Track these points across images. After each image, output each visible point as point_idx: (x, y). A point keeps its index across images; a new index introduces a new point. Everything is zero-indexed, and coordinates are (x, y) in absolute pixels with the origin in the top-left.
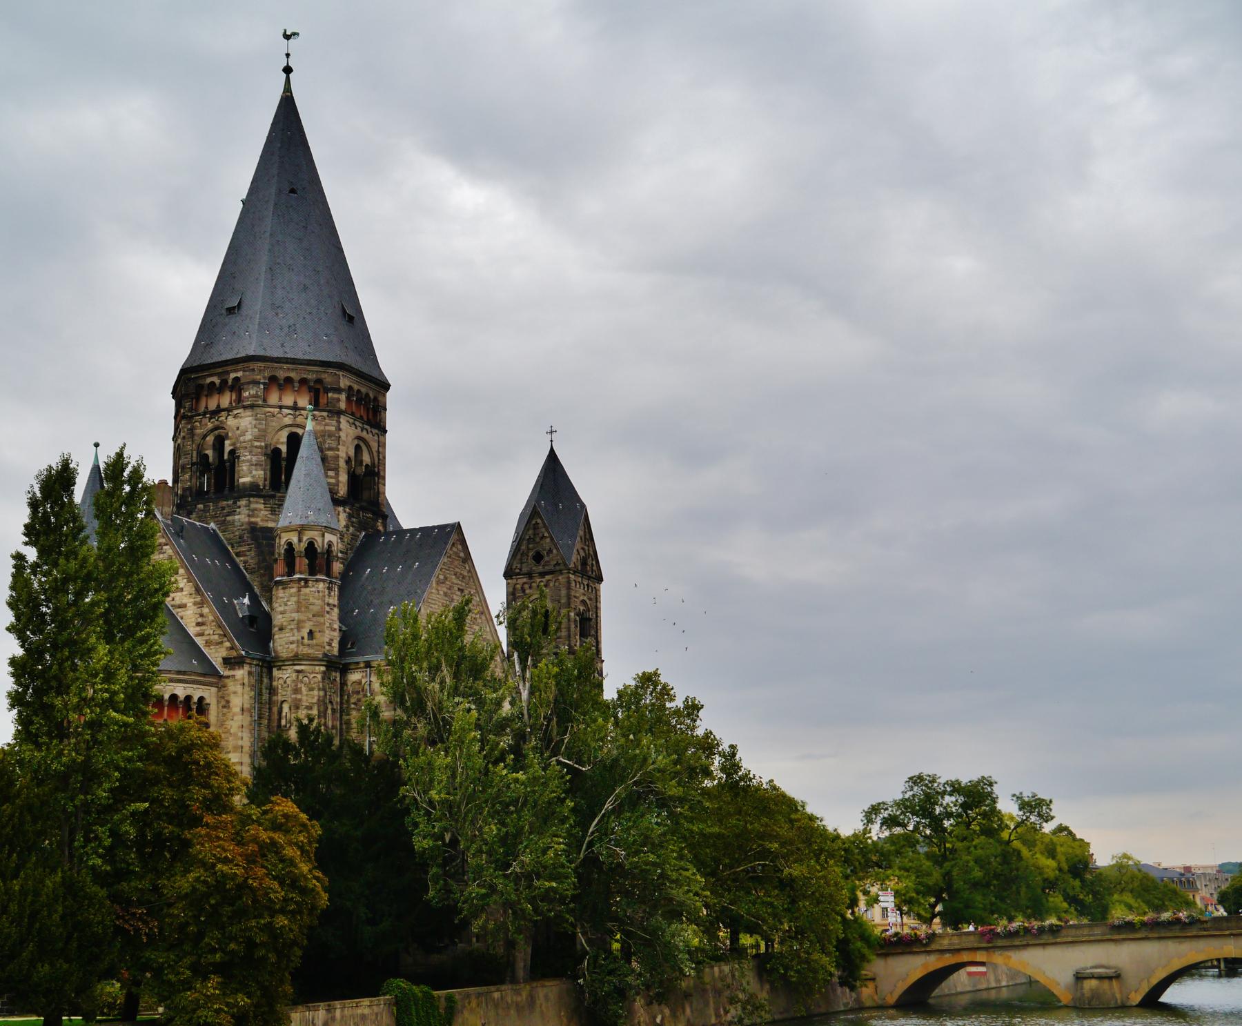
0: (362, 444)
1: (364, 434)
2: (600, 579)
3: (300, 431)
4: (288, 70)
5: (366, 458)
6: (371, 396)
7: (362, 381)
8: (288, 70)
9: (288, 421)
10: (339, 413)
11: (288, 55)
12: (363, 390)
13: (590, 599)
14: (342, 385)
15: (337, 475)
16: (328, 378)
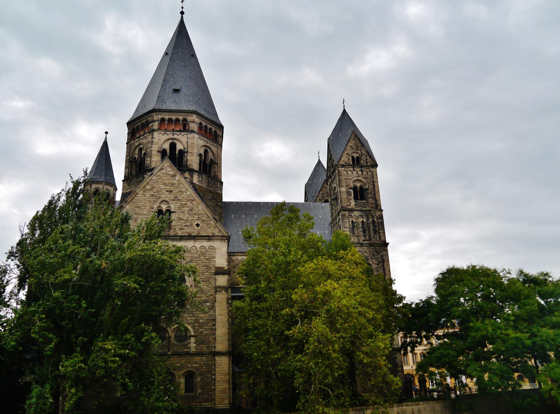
0: (175, 141)
1: (175, 136)
2: (375, 165)
3: (142, 146)
4: (182, 13)
5: (179, 147)
6: (181, 118)
7: (173, 114)
8: (182, 13)
9: (137, 144)
10: (154, 130)
11: (182, 8)
12: (174, 117)
13: (366, 178)
14: (155, 118)
15: (151, 159)
16: (150, 119)
